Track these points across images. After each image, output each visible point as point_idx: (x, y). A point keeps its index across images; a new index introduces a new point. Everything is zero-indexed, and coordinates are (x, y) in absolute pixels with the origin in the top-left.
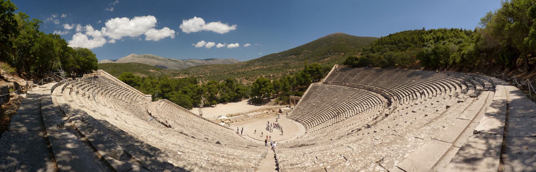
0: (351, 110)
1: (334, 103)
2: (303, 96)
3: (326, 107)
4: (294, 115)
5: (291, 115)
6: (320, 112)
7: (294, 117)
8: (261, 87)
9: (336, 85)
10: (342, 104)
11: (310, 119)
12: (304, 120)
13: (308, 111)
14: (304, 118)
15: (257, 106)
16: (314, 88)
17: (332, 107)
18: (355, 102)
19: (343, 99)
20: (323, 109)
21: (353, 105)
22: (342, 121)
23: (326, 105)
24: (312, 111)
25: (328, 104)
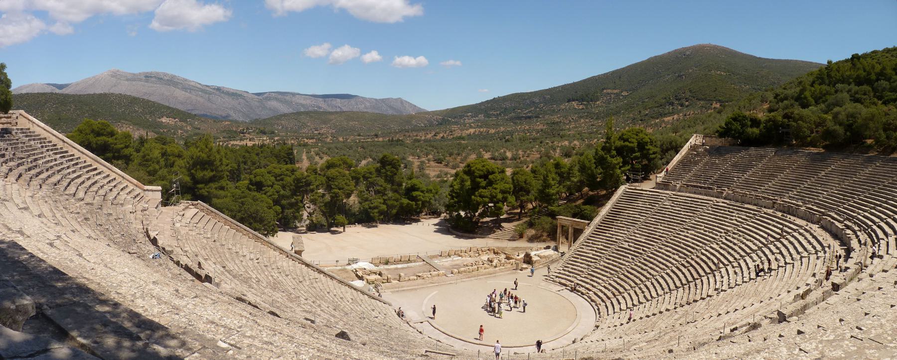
0: (733, 267)
1: (684, 244)
2: (597, 220)
3: (660, 254)
4: (567, 273)
5: (560, 273)
6: (642, 269)
7: (566, 279)
8: (475, 187)
9: (695, 193)
11: (610, 288)
12: (594, 290)
13: (608, 263)
14: (595, 284)
15: (462, 240)
16: (631, 197)
17: (676, 257)
18: (746, 245)
19: (711, 235)
20: (652, 260)
21: (738, 253)
22: (703, 299)
23: (661, 248)
24: (620, 263)
25: (667, 246)
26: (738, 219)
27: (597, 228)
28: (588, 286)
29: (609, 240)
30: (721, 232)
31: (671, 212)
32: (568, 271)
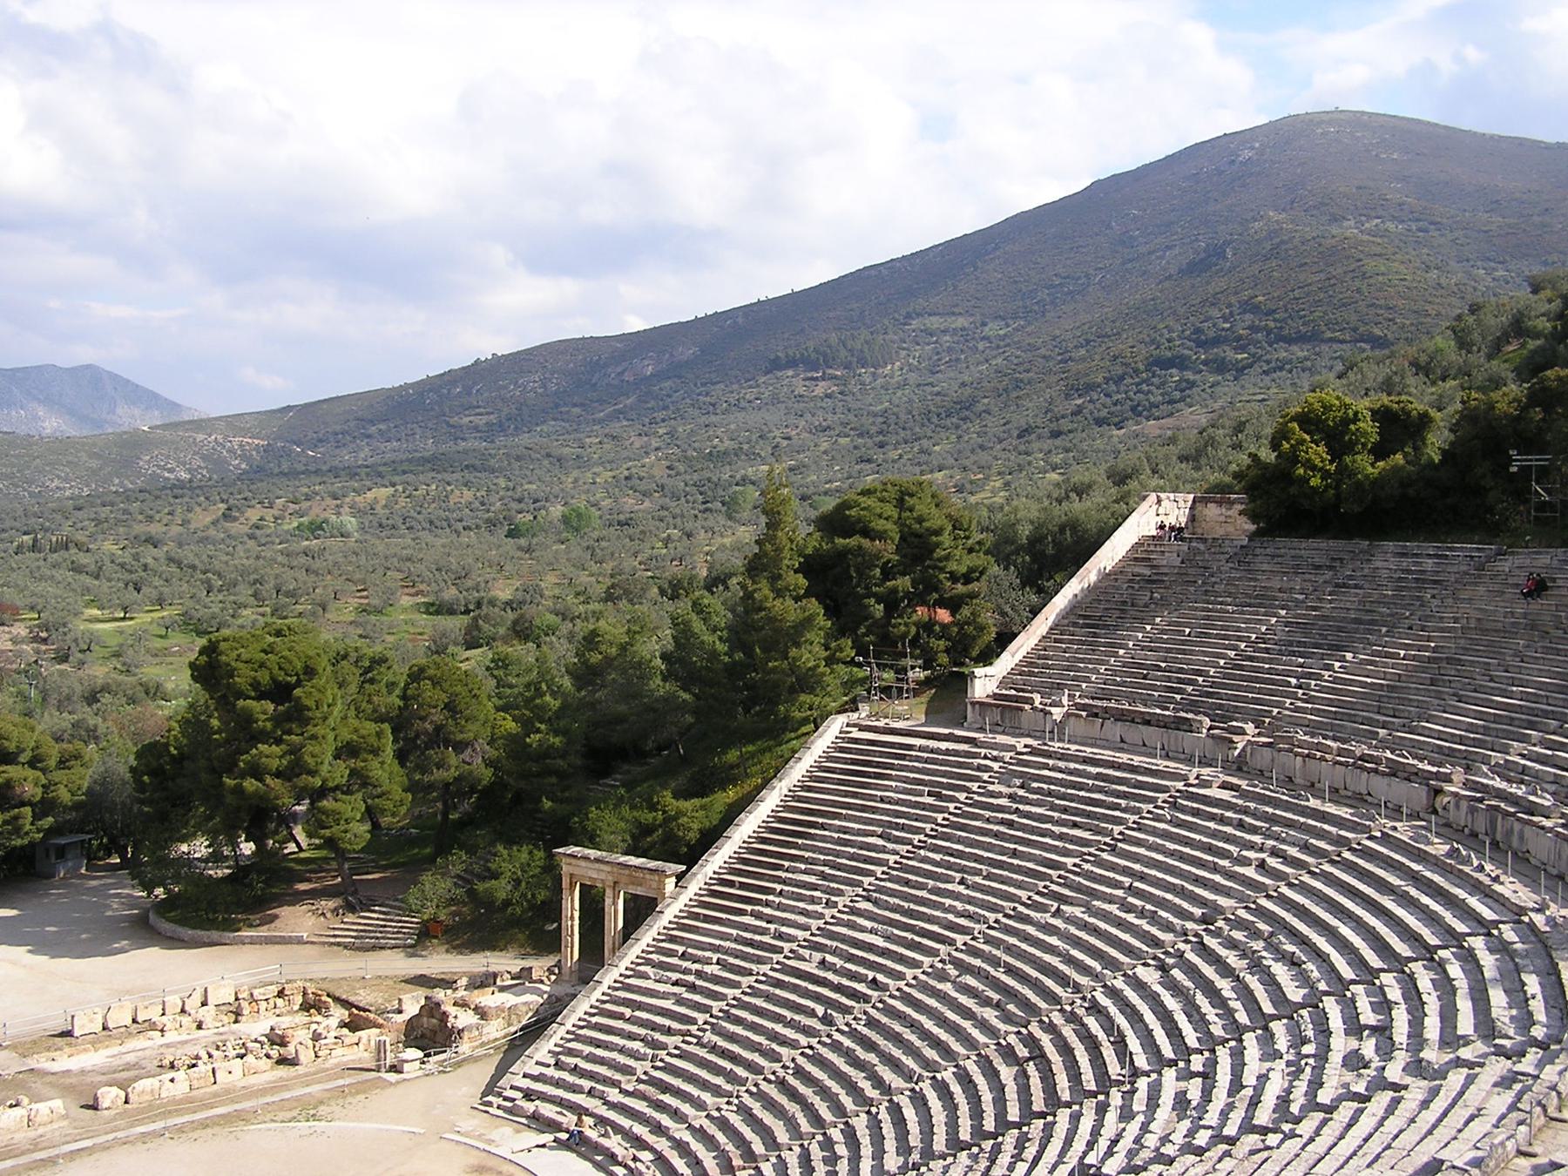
2: (716, 860)
7: (560, 1102)
10: (1119, 983)
12: (662, 1144)
14: (665, 1120)
19: (1143, 924)
26: (1272, 862)
27: (714, 894)
28: (640, 1130)
29: (750, 943)
30: (1188, 916)
31: (1010, 824)
32: (575, 1070)
